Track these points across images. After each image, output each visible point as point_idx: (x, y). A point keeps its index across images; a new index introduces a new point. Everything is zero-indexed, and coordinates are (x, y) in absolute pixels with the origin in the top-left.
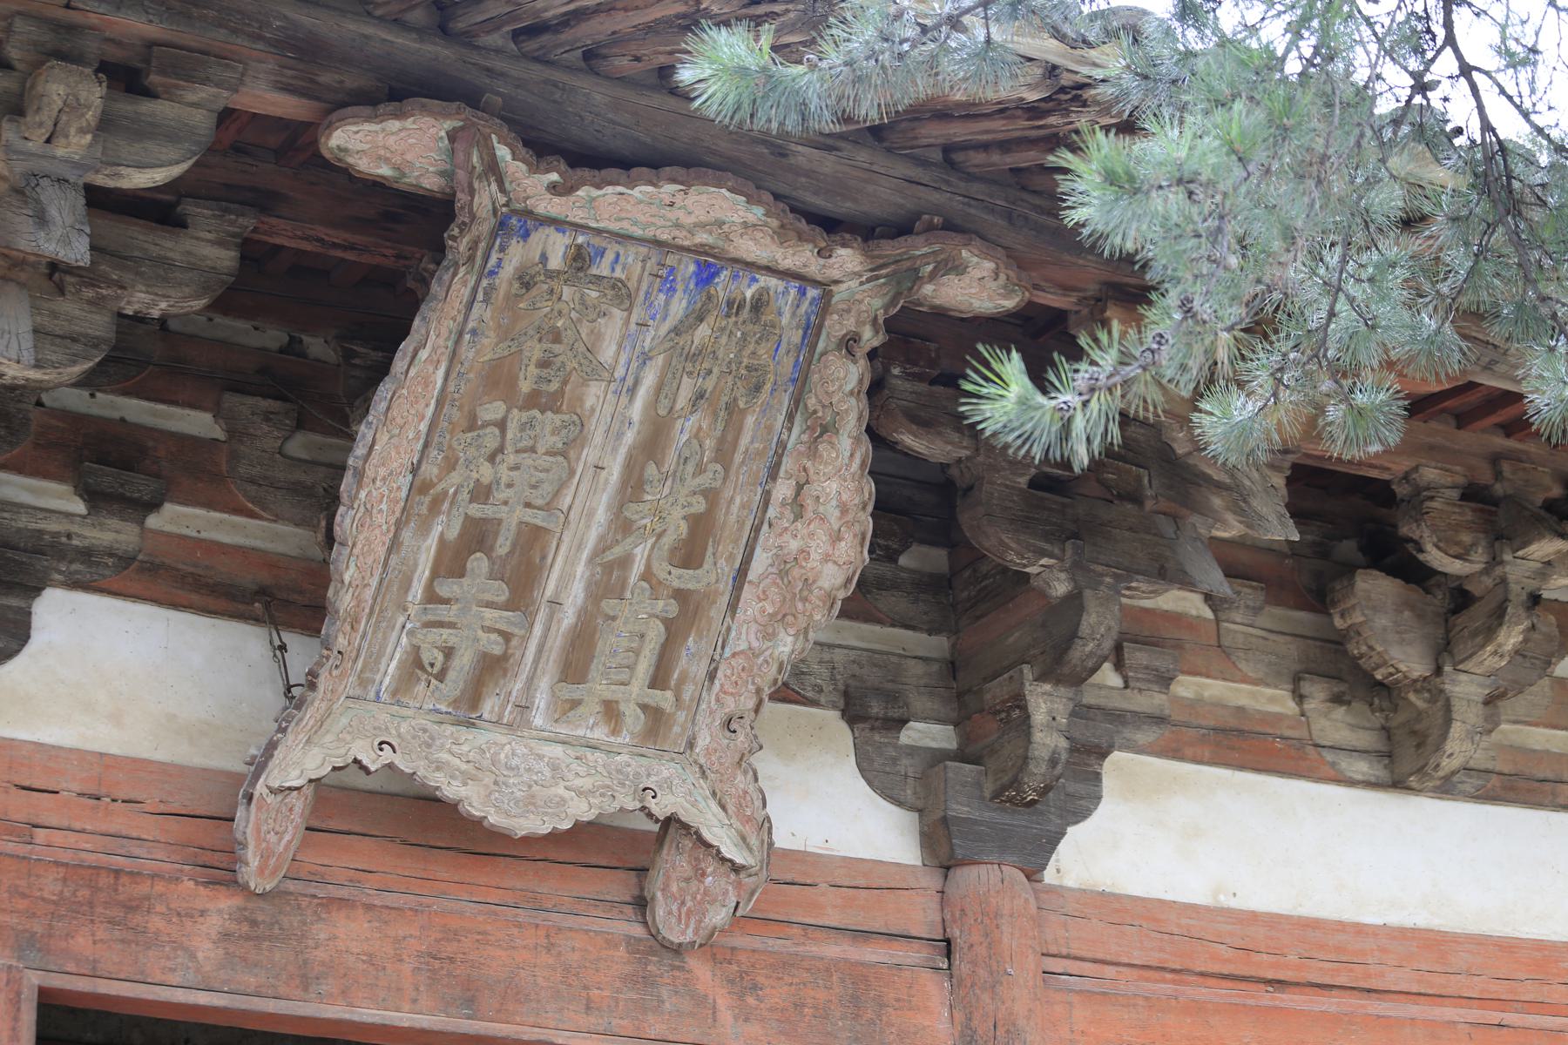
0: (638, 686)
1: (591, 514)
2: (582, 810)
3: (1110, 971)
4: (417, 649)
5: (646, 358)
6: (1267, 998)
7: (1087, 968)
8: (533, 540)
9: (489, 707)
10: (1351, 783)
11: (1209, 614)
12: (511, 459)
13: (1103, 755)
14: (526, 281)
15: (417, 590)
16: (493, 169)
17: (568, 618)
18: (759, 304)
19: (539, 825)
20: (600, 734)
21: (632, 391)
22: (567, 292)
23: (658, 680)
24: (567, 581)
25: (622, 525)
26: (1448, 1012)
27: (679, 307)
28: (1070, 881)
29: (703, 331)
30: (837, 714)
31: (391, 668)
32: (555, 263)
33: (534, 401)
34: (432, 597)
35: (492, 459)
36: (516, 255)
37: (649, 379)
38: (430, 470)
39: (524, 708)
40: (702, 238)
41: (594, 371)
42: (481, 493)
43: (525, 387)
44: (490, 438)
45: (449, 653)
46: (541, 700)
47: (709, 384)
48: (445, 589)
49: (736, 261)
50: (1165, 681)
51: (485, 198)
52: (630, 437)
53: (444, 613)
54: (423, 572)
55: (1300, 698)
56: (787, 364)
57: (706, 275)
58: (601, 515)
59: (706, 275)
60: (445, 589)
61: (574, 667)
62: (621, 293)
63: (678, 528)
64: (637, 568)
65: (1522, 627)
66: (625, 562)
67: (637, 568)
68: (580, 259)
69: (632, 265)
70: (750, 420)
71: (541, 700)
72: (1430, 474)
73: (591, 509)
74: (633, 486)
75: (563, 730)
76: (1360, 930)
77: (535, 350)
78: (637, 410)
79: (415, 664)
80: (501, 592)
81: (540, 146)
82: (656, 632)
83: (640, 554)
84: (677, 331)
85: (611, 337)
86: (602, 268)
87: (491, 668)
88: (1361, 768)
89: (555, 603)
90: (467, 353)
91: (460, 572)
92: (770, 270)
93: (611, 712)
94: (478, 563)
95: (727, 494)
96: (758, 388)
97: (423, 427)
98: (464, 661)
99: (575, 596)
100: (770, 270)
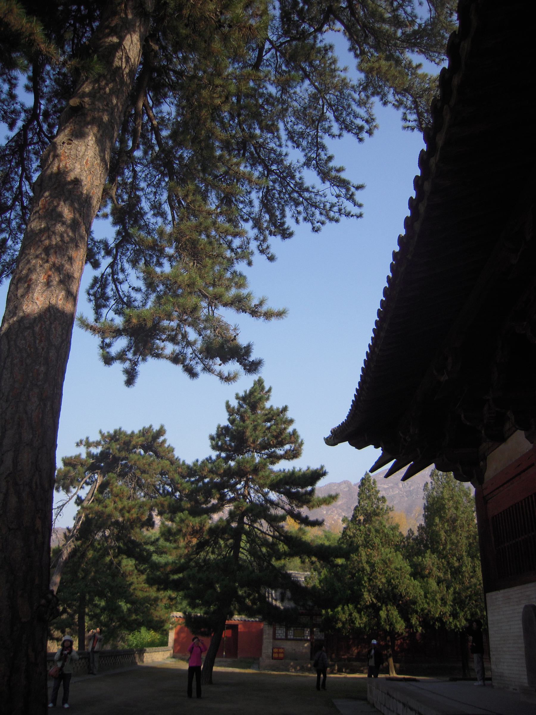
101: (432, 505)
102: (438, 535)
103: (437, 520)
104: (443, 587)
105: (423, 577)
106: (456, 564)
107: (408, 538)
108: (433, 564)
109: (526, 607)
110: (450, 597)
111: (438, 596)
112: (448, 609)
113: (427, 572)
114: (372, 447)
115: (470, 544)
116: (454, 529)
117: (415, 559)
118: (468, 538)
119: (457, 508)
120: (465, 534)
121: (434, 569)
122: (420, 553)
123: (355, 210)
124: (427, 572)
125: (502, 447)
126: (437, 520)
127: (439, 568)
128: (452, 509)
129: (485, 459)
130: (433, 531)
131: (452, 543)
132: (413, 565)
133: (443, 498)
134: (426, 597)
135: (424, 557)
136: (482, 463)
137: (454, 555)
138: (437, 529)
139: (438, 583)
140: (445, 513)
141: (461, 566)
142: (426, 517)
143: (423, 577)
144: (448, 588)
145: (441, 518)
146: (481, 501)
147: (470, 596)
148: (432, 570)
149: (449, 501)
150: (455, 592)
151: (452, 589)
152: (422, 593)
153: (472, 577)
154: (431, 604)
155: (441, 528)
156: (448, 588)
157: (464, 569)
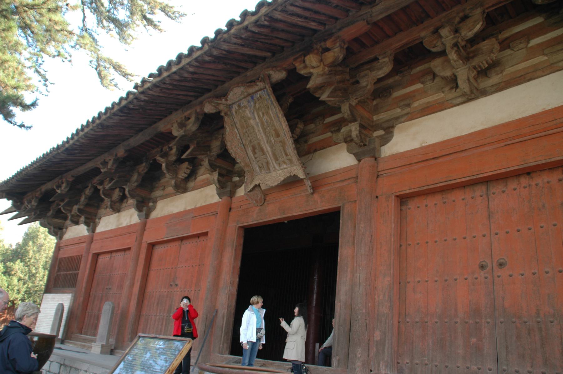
0: (285, 157)
1: (262, 137)
2: (282, 179)
3: (394, 170)
4: (259, 166)
5: (253, 113)
6: (432, 162)
7: (389, 171)
8: (259, 144)
9: (271, 169)
10: (458, 105)
11: (422, 86)
12: (250, 135)
13: (393, 127)
14: (236, 113)
15: (253, 158)
16: (218, 104)
17: (270, 153)
18: (260, 97)
19: (276, 184)
20: (285, 166)
21: (255, 118)
22: (241, 111)
23: (287, 155)
24: (267, 148)
25: (267, 137)
26: (487, 148)
27: (252, 104)
28: (387, 155)
29: (257, 105)
30: (344, 143)
31: (258, 169)
32: (237, 108)
33: (247, 127)
34: (256, 158)
35: (248, 136)
36: (234, 110)
37: (256, 115)
38: (244, 142)
39: (274, 167)
40: (246, 94)
41: (250, 119)
42: (251, 142)
43: (245, 125)
44: (247, 135)
45: (262, 164)
46: (275, 165)
47: (263, 110)
48: (256, 156)
49: (253, 93)
50: (409, 105)
51: (221, 107)
52: (259, 125)
53: (258, 159)
54: (252, 155)
55: (443, 92)
56: (270, 102)
57: (252, 98)
58: (264, 136)
59: (252, 98)
60: (256, 156)
61: (276, 159)
62: (245, 107)
63: (273, 133)
64: (273, 141)
65: (453, 53)
66: (271, 141)
67: (273, 141)
68: (239, 106)
69: (244, 103)
70: (271, 112)
71: (275, 165)
72: (423, 34)
73: (261, 136)
74: (264, 130)
75: (281, 168)
76: (458, 138)
77: (243, 120)
78: (258, 120)
79: (260, 167)
80: (261, 153)
81: (219, 97)
82: (281, 148)
83: (272, 139)
84: (255, 107)
85: (248, 113)
86: (242, 105)
87: (268, 163)
88: (460, 100)
89: (267, 151)
90: (237, 126)
91: (256, 153)
92: (257, 91)
93: (284, 162)
94: (257, 151)
95: (275, 124)
96: (268, 108)
97: (238, 137)
98: (264, 164)
99: (269, 149)
100: (257, 91)
101: (30, 234)
102: (28, 252)
103: (31, 243)
104: (21, 283)
105: (9, 275)
106: (34, 271)
107: (7, 250)
108: (19, 269)
109: (59, 304)
110: (24, 290)
111: (16, 288)
112: (20, 296)
113: (13, 273)
114: (6, 199)
115: (46, 262)
116: (39, 251)
117: (8, 264)
118: (46, 258)
119: (45, 239)
120: (45, 255)
121: (19, 272)
122: (13, 260)
123: (47, 93)
124: (13, 273)
125: (76, 227)
126: (31, 243)
127: (22, 272)
128: (42, 239)
129: (67, 228)
130: (26, 249)
131: (36, 259)
132: (5, 267)
133: (38, 231)
134: (8, 287)
135: (14, 263)
136: (64, 230)
137: (34, 266)
138: (29, 248)
139: (19, 281)
140: (37, 240)
141: (36, 273)
142: (24, 239)
143: (9, 275)
144: (24, 284)
145: (34, 242)
146: (58, 248)
147: (36, 291)
148: (17, 272)
149: (42, 234)
150: (27, 287)
151: (26, 285)
152: (6, 285)
153: (41, 281)
154: (10, 292)
155: (31, 248)
156: (24, 284)
157: (37, 275)
